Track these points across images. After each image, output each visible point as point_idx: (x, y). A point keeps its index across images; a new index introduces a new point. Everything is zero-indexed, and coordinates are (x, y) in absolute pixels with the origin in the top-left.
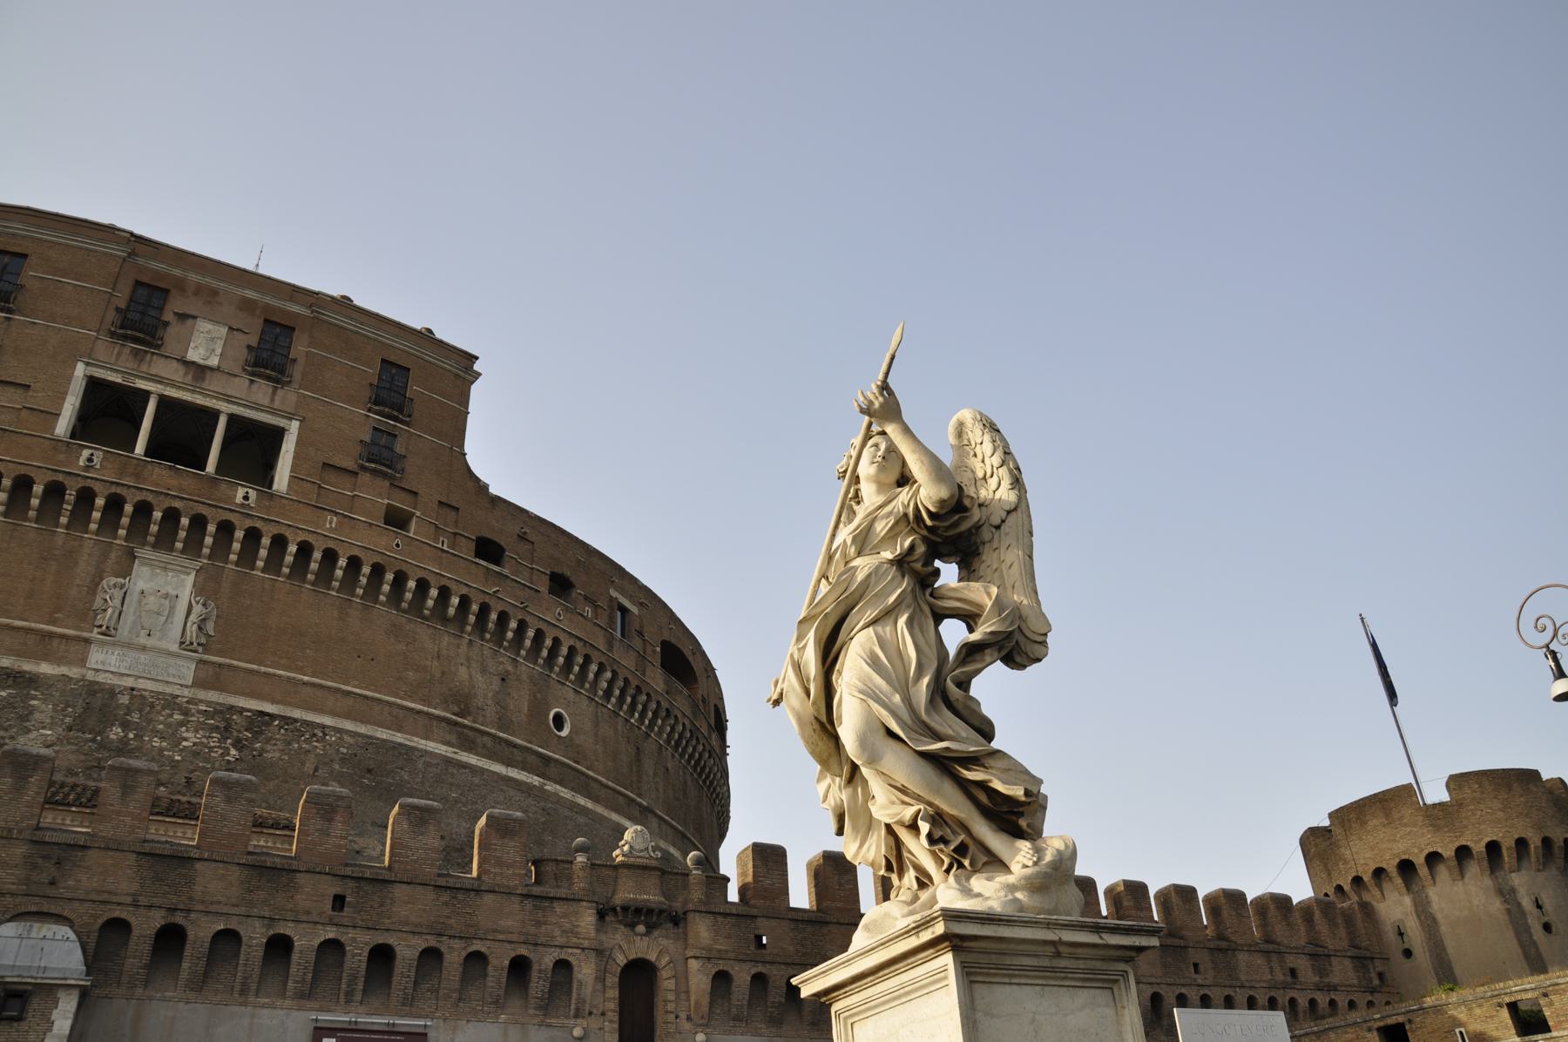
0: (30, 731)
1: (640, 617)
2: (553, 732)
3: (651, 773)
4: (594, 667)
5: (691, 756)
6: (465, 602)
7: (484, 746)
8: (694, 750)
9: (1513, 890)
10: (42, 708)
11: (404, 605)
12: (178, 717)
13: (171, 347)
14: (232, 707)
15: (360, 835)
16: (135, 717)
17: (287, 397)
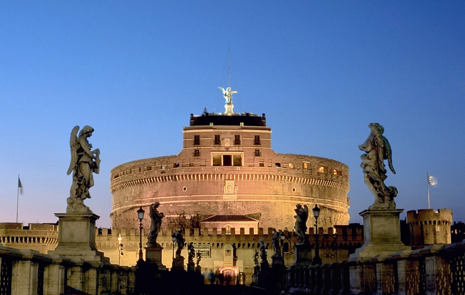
0: (218, 209)
1: (310, 163)
2: (292, 192)
3: (315, 191)
4: (300, 178)
5: (326, 184)
6: (274, 176)
7: (280, 198)
8: (327, 183)
9: (423, 228)
10: (219, 206)
11: (265, 179)
12: (236, 204)
13: (222, 145)
14: (242, 201)
15: (263, 216)
16: (230, 205)
17: (241, 149)
